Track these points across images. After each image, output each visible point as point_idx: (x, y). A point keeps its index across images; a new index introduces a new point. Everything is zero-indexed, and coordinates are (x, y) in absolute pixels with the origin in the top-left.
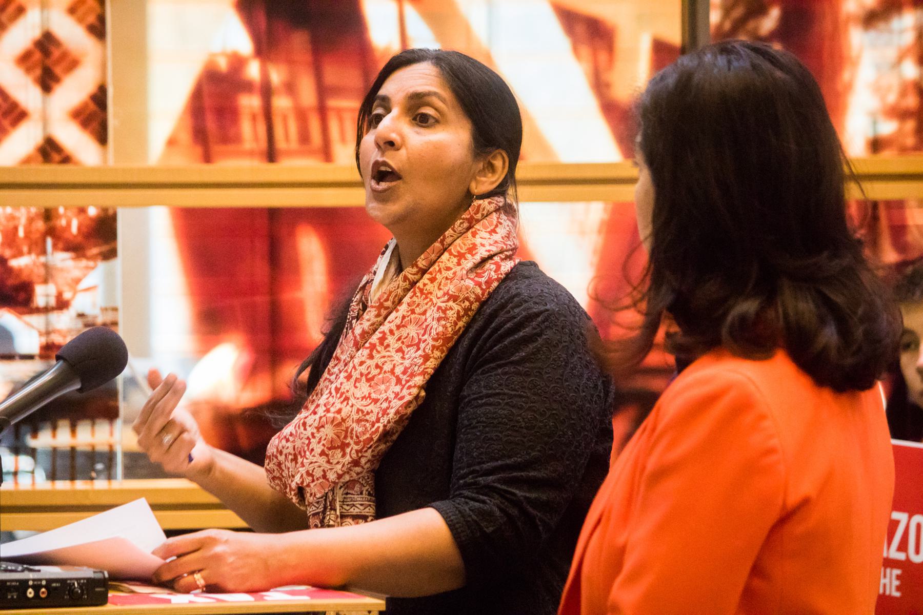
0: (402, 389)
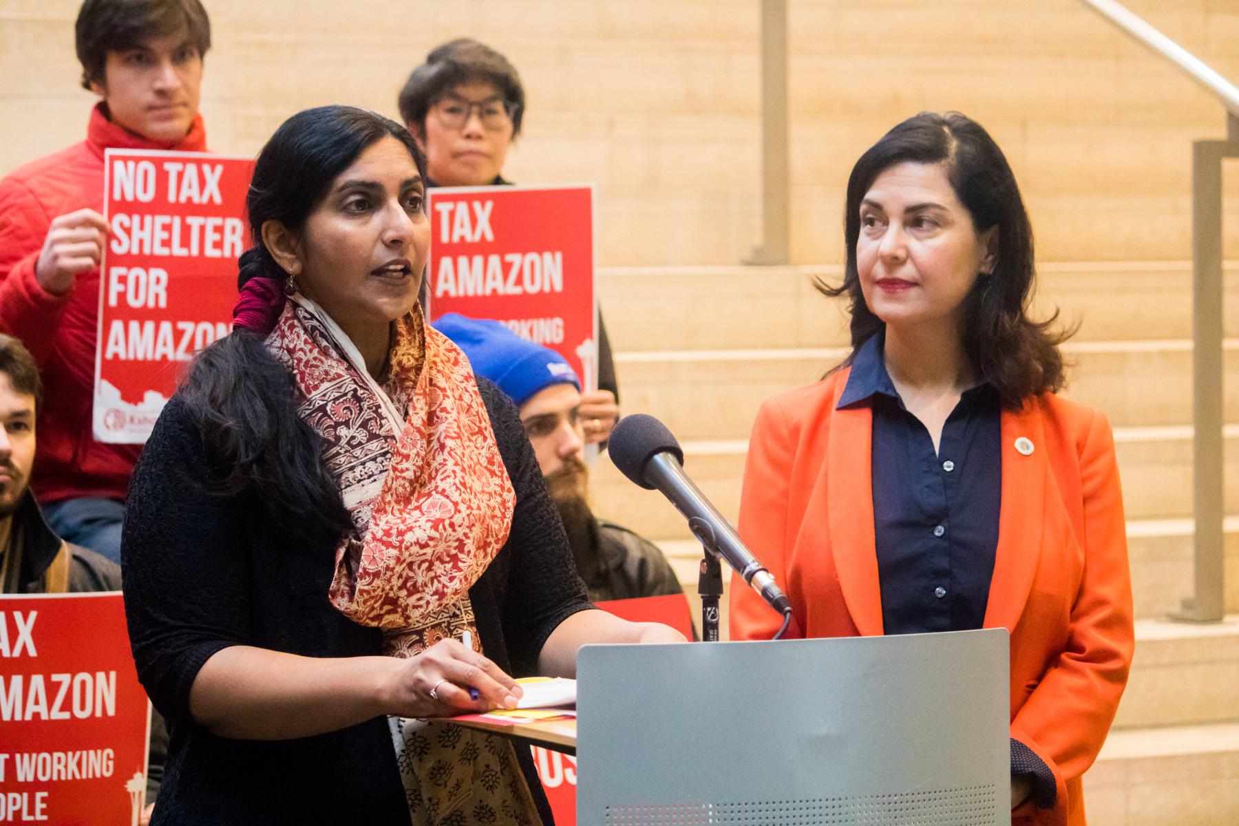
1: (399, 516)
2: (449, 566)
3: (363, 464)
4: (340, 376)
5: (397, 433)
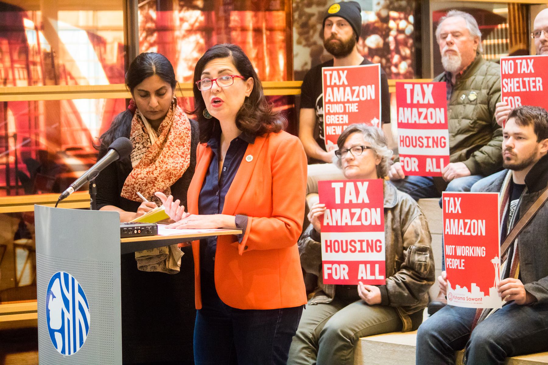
0: (185, 159)
2: (152, 185)
3: (140, 155)
4: (139, 129)
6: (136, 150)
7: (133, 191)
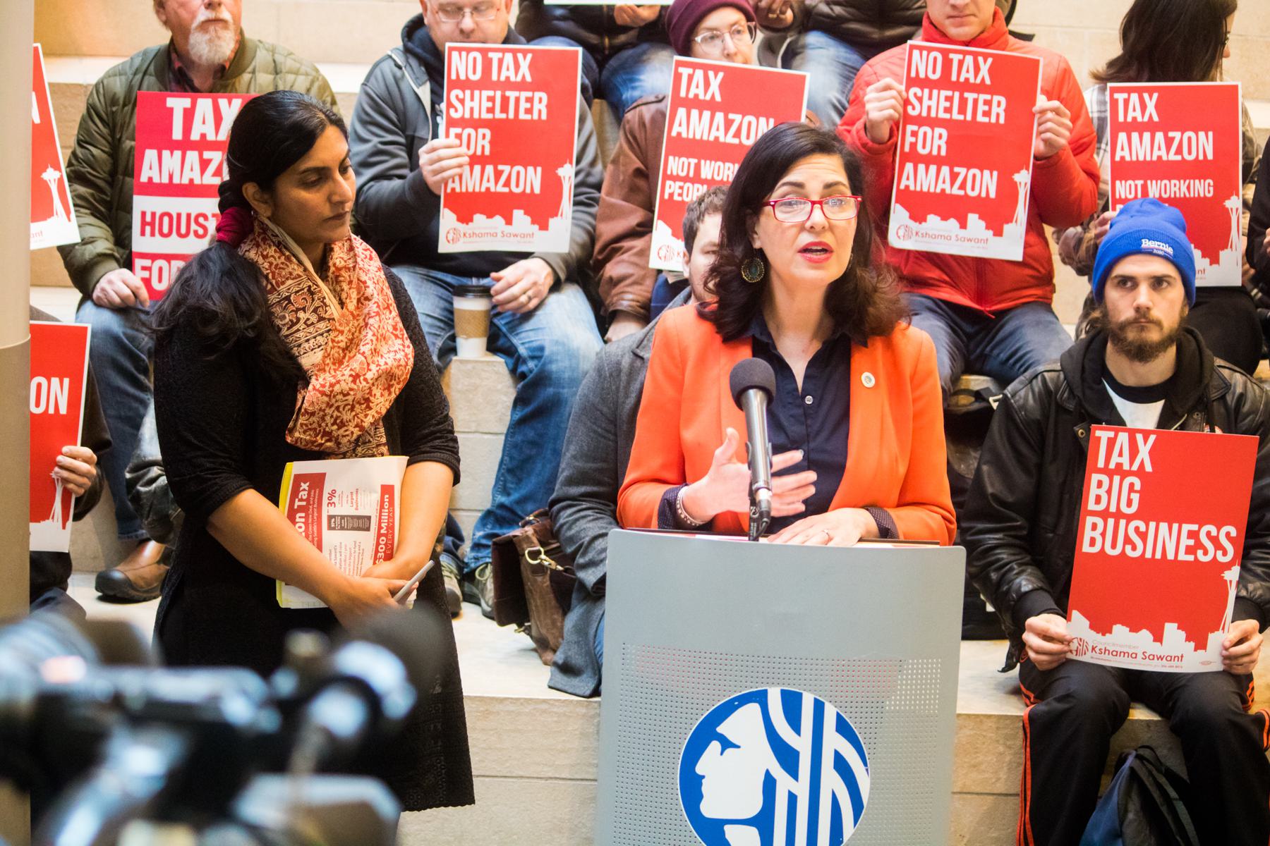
1: (333, 373)
2: (364, 406)
3: (315, 337)
4: (300, 276)
5: (336, 316)
6: (301, 325)
7: (320, 426)
